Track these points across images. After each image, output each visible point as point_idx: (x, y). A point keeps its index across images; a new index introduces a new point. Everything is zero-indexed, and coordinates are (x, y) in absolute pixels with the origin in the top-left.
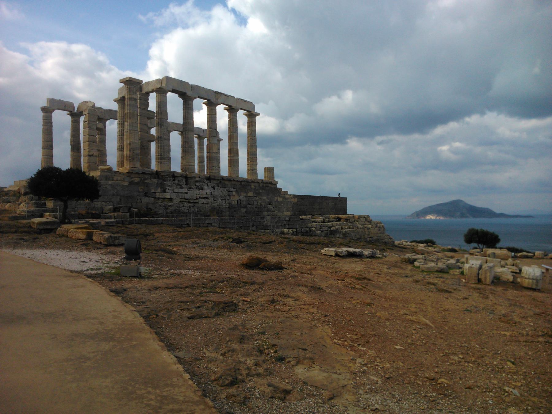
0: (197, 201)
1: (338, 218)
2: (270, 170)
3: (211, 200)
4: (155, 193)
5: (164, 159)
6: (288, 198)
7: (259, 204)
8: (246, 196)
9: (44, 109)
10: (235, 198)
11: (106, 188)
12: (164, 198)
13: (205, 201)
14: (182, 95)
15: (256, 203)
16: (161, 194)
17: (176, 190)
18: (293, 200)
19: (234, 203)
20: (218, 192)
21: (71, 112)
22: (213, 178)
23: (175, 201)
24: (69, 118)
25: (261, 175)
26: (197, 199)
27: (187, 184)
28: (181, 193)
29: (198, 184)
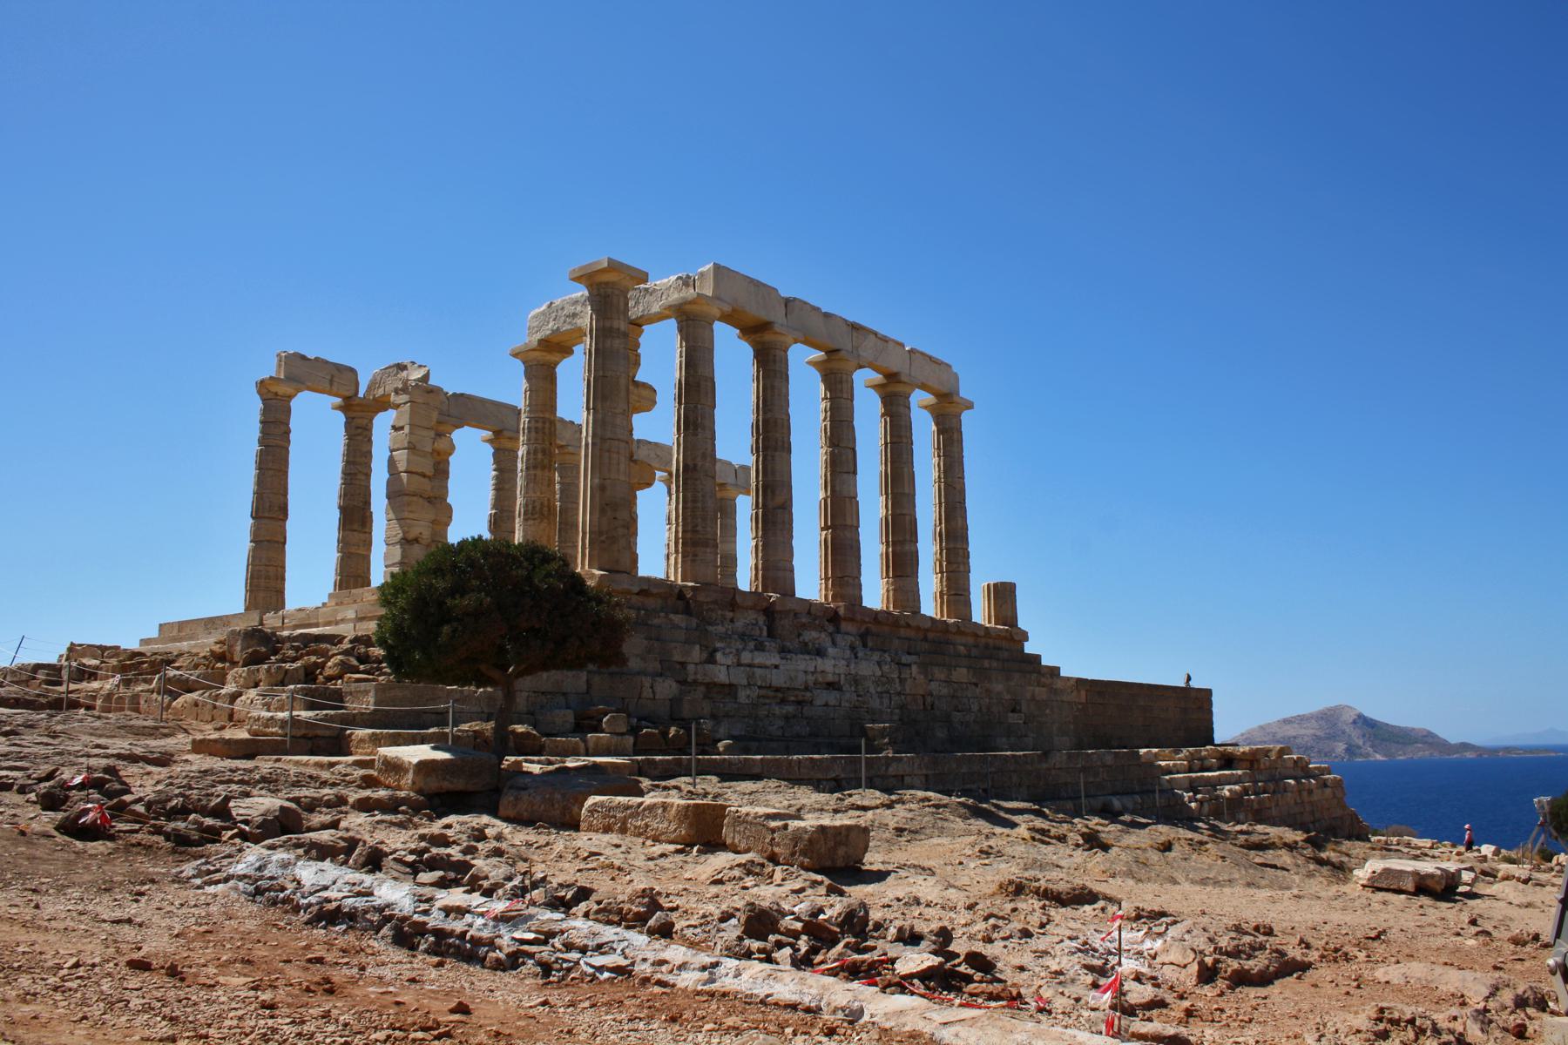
0: (808, 694)
8: (948, 682)
9: (262, 386)
13: (831, 697)
15: (975, 708)
17: (746, 657)
21: (346, 399)
23: (743, 696)
24: (340, 418)
27: (771, 635)
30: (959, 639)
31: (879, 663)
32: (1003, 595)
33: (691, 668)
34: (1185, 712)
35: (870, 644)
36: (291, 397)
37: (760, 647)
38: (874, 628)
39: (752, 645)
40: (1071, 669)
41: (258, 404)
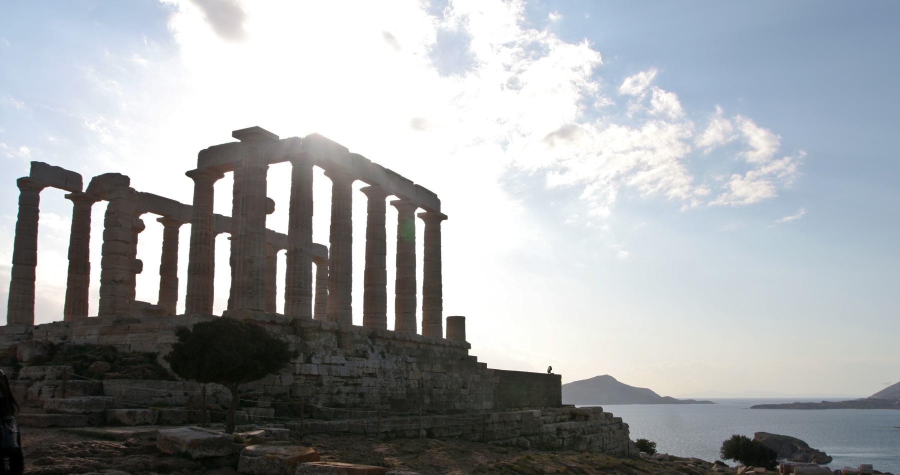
2: (458, 323)
3: (380, 379)
8: (431, 372)
9: (21, 183)
10: (415, 375)
15: (444, 386)
17: (327, 360)
19: (414, 385)
22: (380, 334)
23: (325, 381)
24: (70, 204)
26: (359, 377)
27: (339, 346)
28: (335, 364)
30: (436, 349)
33: (298, 366)
35: (391, 351)
36: (41, 189)
37: (334, 353)
38: (393, 342)
39: (330, 352)
41: (18, 192)
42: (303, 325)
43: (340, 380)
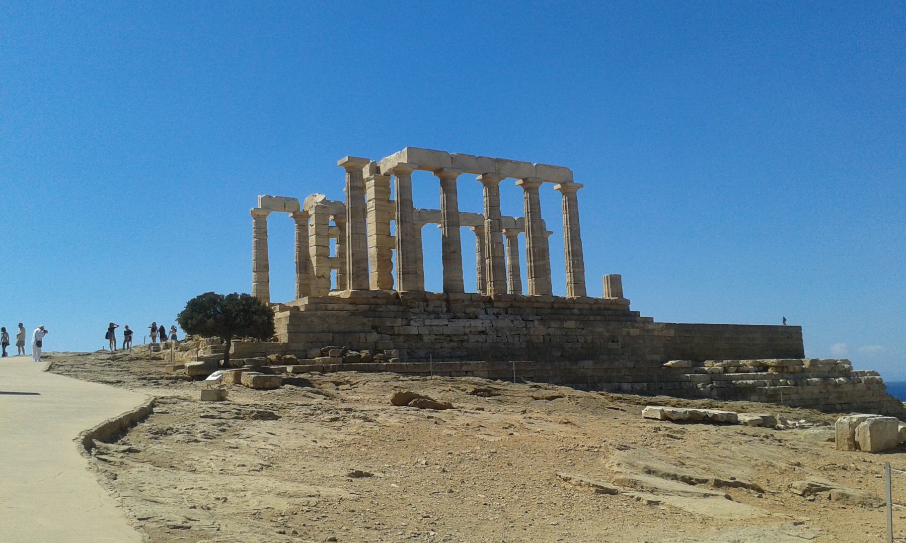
0: (466, 337)
1: (761, 364)
4: (393, 327)
5: (408, 273)
6: (653, 330)
7: (589, 341)
8: (562, 328)
11: (312, 321)
12: (409, 335)
13: (481, 338)
14: (438, 171)
15: (582, 340)
16: (402, 328)
17: (428, 322)
18: (665, 333)
20: (504, 323)
23: (426, 339)
25: (597, 290)
26: (465, 334)
27: (448, 311)
29: (468, 310)
31: (512, 321)
32: (615, 281)
34: (784, 341)
35: (510, 312)
40: (660, 318)
42: (406, 297)
43: (442, 337)
